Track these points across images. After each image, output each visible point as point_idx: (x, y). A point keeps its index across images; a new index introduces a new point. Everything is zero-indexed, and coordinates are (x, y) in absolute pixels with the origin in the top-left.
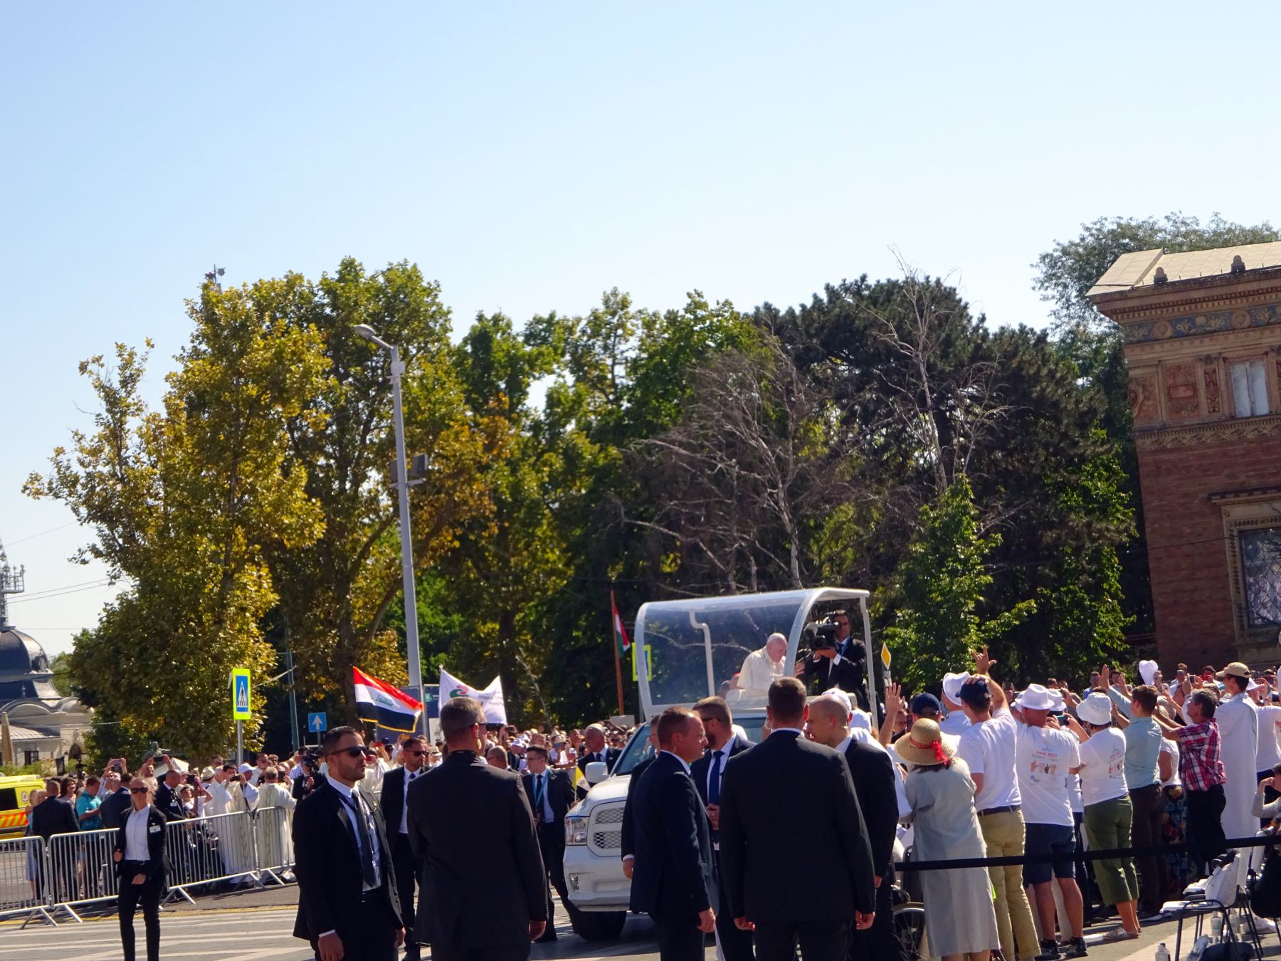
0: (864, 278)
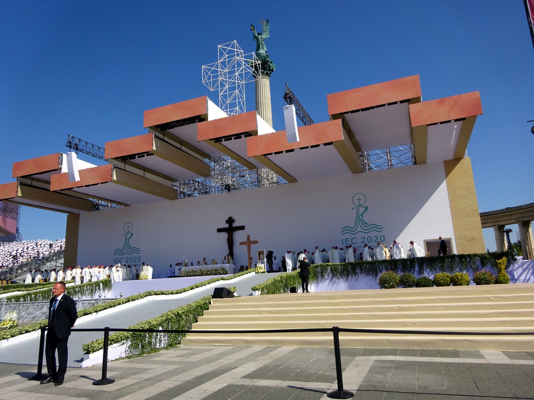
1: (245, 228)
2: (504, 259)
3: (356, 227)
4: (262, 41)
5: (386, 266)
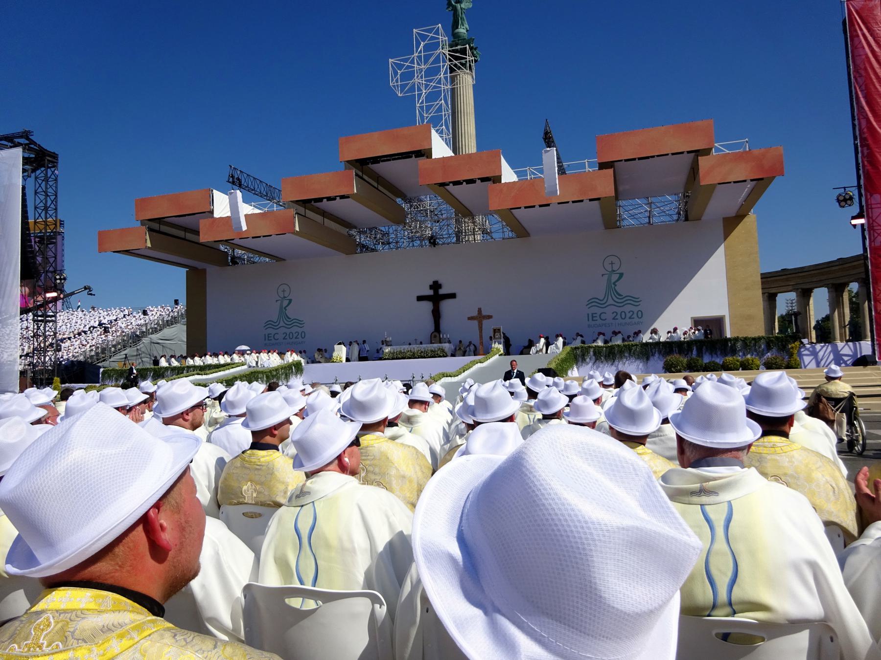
1: (457, 295)
3: (606, 298)
4: (462, 14)
5: (659, 348)
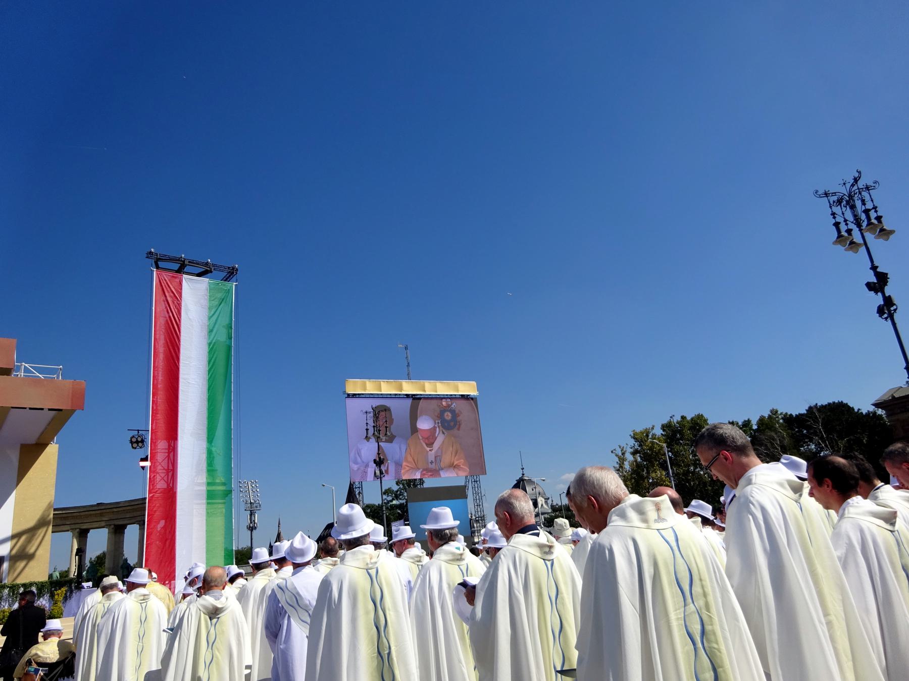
0: (817, 404)
2: (64, 589)
